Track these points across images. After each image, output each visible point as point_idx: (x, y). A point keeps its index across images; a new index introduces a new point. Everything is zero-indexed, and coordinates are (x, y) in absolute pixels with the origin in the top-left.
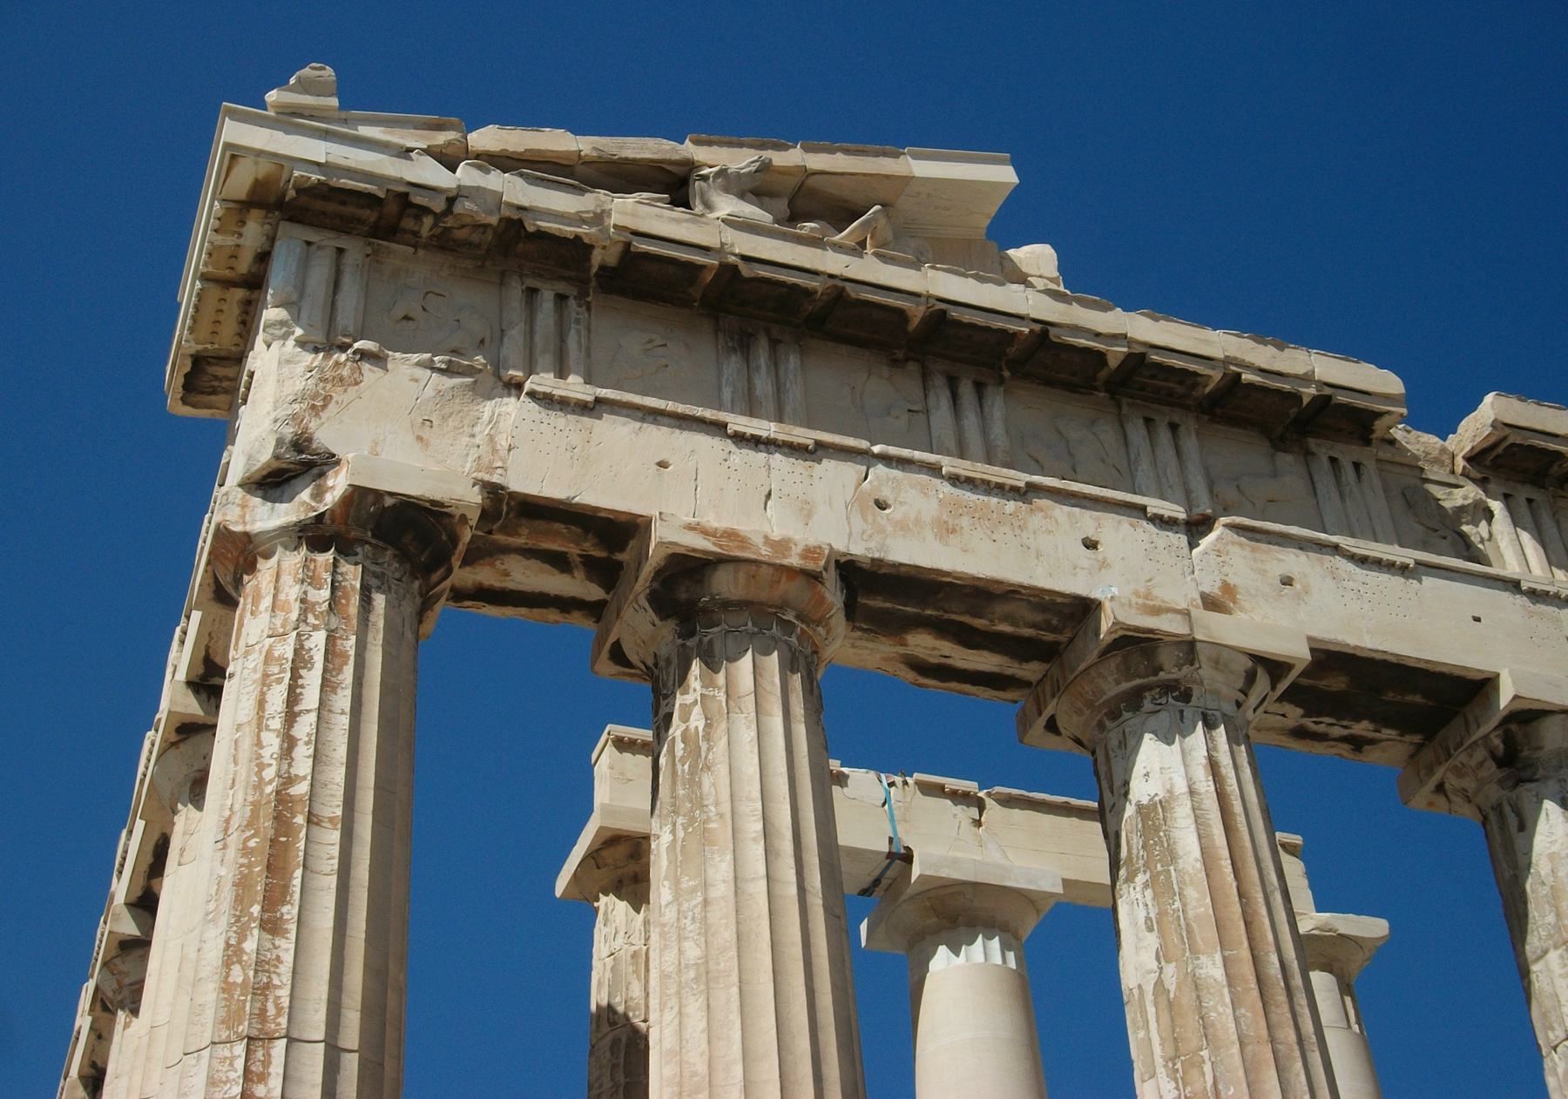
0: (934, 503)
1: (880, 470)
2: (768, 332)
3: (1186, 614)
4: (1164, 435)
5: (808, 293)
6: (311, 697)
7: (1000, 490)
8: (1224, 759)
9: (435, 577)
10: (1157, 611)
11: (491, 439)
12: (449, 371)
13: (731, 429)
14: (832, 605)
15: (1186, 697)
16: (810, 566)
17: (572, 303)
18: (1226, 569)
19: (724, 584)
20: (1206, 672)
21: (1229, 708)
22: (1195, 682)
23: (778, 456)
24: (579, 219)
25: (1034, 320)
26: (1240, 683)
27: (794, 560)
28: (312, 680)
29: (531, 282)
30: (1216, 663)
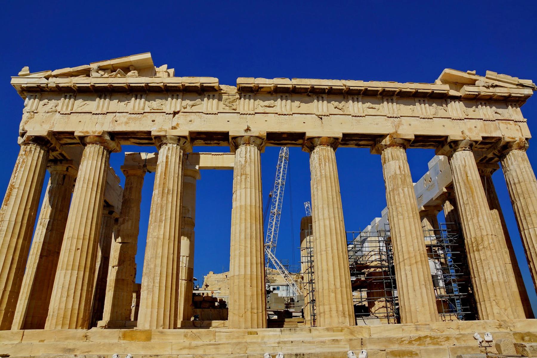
3: (166, 131)
5: (106, 87)
6: (19, 169)
8: (170, 155)
10: (160, 131)
27: (96, 134)
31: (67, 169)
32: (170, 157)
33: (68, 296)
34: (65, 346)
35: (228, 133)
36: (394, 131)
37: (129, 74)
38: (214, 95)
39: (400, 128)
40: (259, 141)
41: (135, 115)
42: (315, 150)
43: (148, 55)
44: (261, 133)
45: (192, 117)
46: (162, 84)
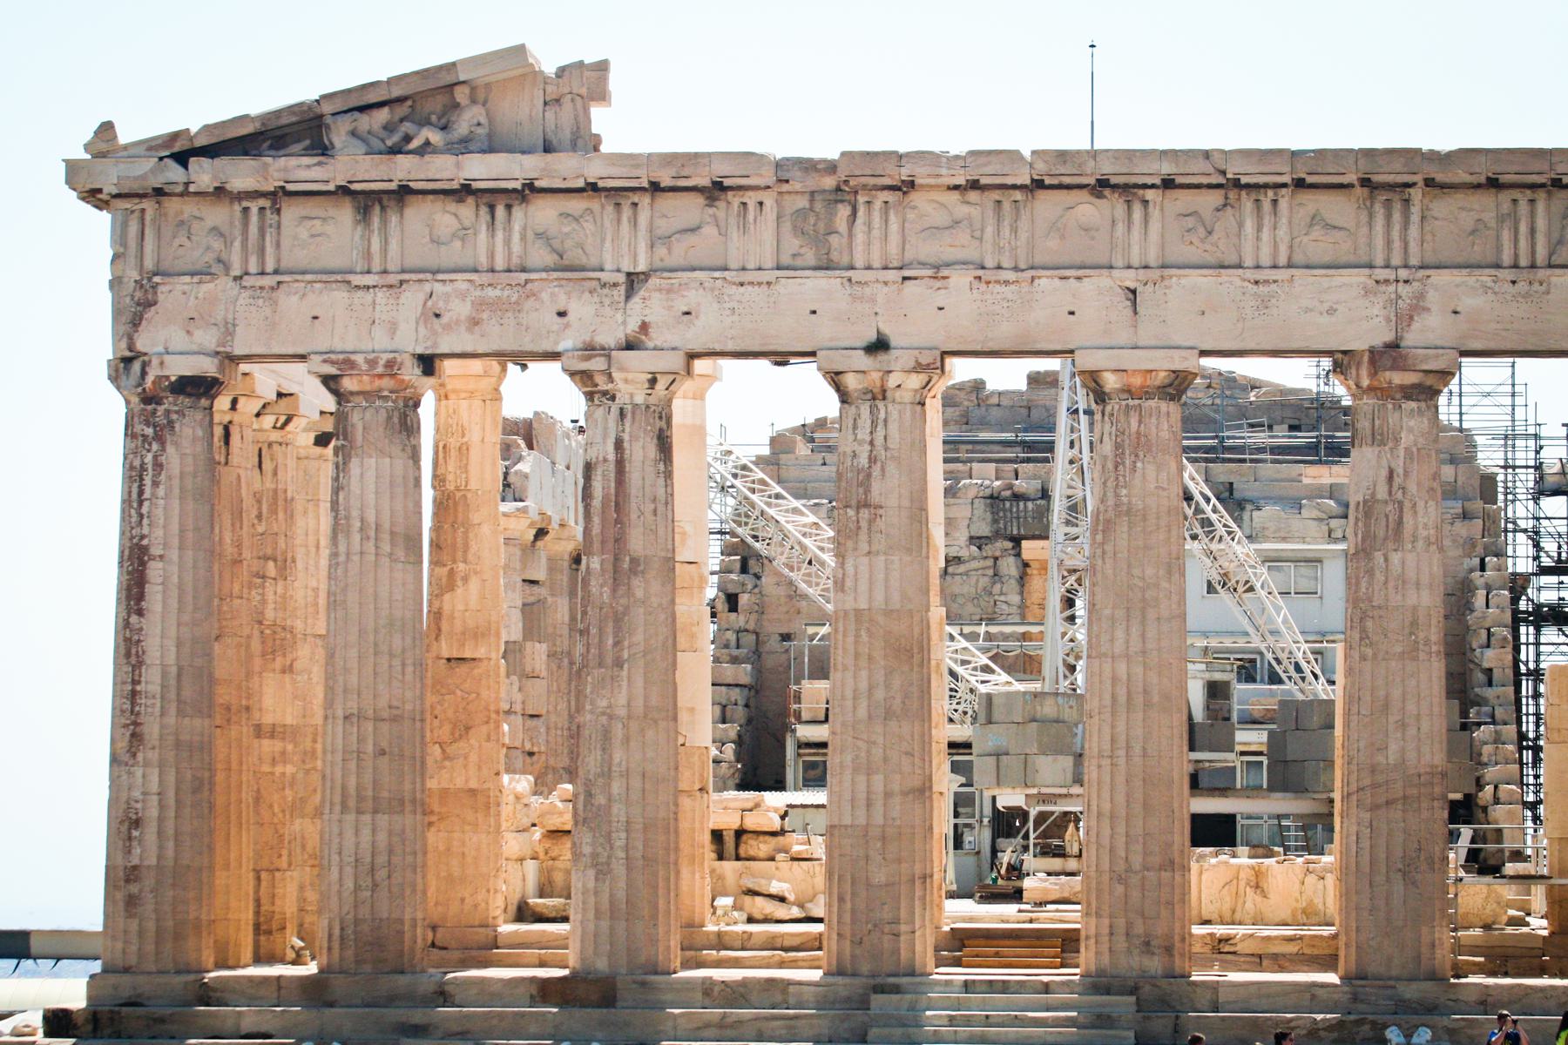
2: (380, 202)
4: (627, 212)
6: (147, 495)
8: (626, 437)
10: (588, 358)
13: (355, 283)
15: (613, 398)
17: (268, 212)
18: (647, 311)
19: (348, 384)
20: (621, 385)
21: (640, 399)
27: (380, 370)
28: (148, 481)
29: (245, 204)
30: (626, 381)
31: (234, 402)
32: (626, 445)
33: (375, 885)
36: (1389, 337)
37: (462, 127)
38: (761, 204)
39: (1416, 325)
40: (915, 381)
41: (498, 292)
42: (1108, 408)
45: (692, 298)
46: (580, 183)
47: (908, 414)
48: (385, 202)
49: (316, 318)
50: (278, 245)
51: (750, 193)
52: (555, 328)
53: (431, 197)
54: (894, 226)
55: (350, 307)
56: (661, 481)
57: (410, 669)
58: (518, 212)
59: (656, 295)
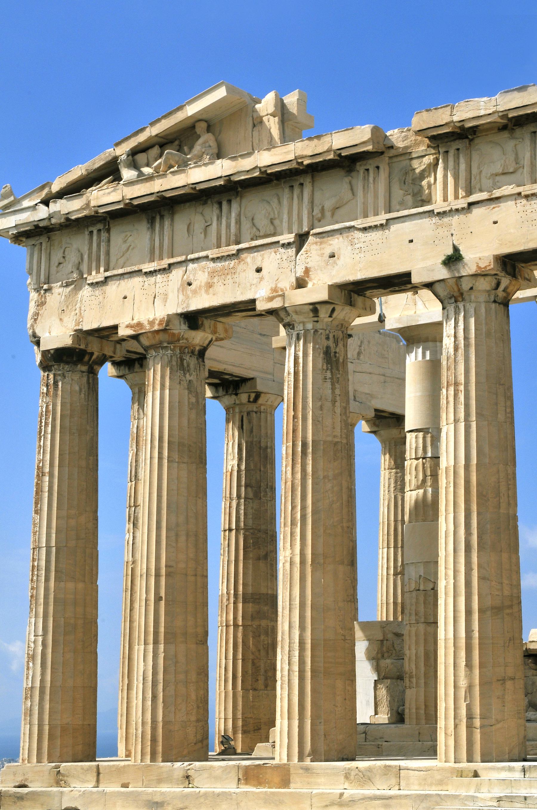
0: (206, 274)
1: (191, 266)
2: (160, 213)
7: (230, 257)
9: (86, 358)
10: (271, 299)
11: (80, 307)
12: (67, 285)
13: (144, 271)
14: (180, 333)
15: (293, 328)
16: (161, 328)
17: (102, 231)
18: (308, 260)
20: (295, 317)
21: (310, 326)
22: (294, 321)
23: (159, 276)
24: (82, 209)
25: (225, 176)
26: (311, 315)
27: (156, 328)
29: (91, 229)
30: (296, 312)
32: (301, 360)
34: (150, 798)
35: (408, 275)
37: (197, 148)
38: (378, 167)
43: (221, 93)
44: (482, 265)
45: (336, 243)
47: (483, 310)
48: (162, 213)
49: (125, 298)
50: (108, 253)
51: (370, 161)
52: (255, 281)
53: (188, 204)
54: (463, 166)
55: (143, 288)
56: (328, 385)
57: (183, 538)
58: (235, 206)
59: (314, 247)
